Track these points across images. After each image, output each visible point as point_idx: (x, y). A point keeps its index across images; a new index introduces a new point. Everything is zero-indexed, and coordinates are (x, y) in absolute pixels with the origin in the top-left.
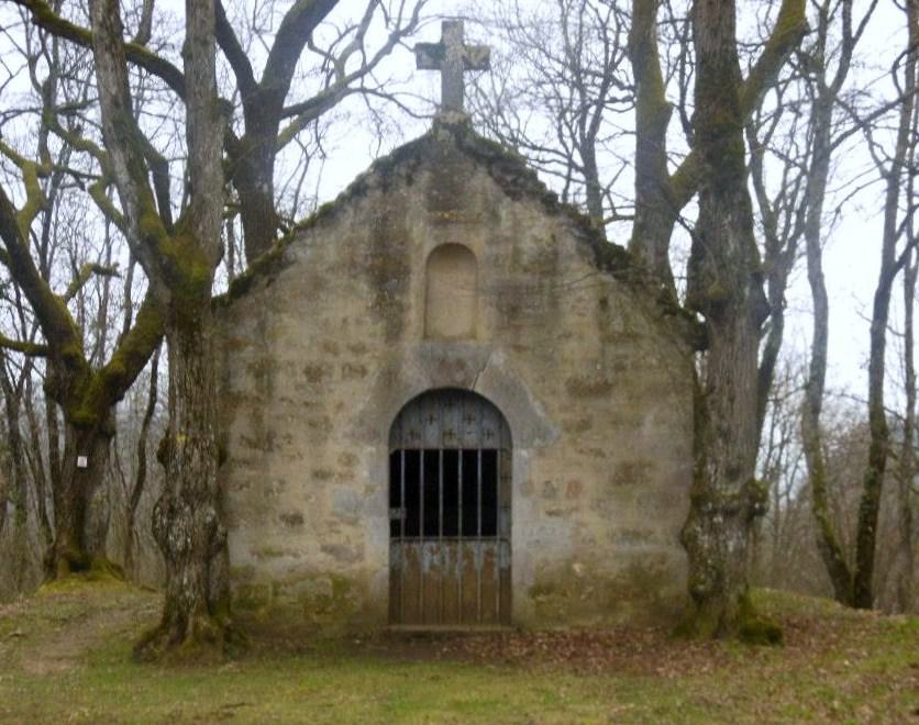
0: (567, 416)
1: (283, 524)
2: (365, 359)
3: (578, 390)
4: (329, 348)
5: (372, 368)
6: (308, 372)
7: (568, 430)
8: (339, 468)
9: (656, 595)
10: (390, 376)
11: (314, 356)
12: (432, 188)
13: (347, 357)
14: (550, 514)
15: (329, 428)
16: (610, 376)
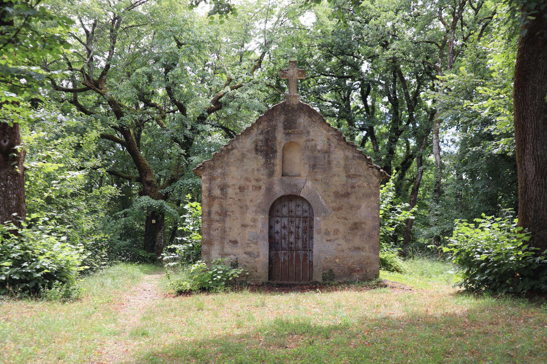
0: (334, 205)
1: (230, 244)
2: (261, 183)
3: (337, 195)
4: (247, 179)
5: (263, 187)
6: (240, 188)
7: (334, 210)
8: (251, 224)
9: (366, 271)
10: (269, 190)
11: (242, 183)
12: (285, 121)
13: (254, 183)
14: (327, 241)
15: (247, 209)
16: (349, 190)
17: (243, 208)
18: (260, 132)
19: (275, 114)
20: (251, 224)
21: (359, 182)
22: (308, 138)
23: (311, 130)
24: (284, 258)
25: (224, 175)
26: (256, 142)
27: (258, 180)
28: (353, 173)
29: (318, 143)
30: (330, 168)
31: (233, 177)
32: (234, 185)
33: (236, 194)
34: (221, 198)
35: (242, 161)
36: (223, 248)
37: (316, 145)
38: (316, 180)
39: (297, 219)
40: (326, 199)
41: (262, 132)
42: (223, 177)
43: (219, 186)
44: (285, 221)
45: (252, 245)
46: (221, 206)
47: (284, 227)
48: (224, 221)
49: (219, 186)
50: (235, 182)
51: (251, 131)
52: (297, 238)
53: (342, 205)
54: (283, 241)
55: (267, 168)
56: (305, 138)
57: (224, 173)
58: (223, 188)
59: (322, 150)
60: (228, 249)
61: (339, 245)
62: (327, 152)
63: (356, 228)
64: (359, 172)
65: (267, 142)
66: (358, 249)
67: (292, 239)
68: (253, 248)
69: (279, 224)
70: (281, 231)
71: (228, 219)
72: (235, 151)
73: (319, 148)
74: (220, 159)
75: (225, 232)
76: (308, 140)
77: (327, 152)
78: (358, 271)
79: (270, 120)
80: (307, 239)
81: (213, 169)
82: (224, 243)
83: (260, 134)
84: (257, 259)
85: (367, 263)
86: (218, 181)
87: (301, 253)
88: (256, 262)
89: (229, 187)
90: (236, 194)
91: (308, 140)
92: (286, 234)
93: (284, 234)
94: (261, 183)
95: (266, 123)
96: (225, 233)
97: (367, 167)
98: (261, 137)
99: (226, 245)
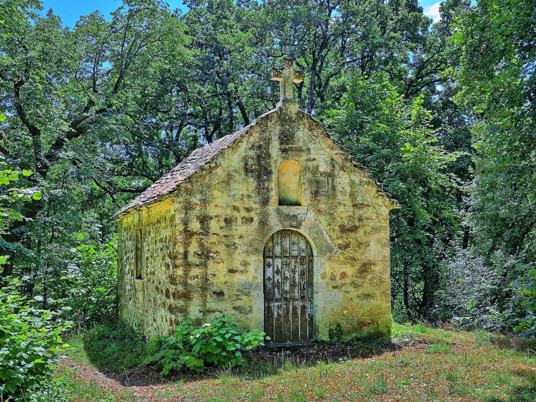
0: (340, 242)
1: (215, 296)
2: (252, 214)
3: (343, 229)
4: (236, 208)
5: (256, 218)
6: (225, 220)
7: (340, 248)
8: (242, 268)
9: (377, 323)
10: (263, 223)
11: (229, 212)
12: (282, 134)
13: (244, 213)
14: (334, 287)
15: (236, 248)
16: (357, 223)
17: (231, 247)
18: (250, 146)
19: (269, 125)
20: (242, 268)
21: (368, 213)
22: (309, 156)
23: (312, 148)
24: (278, 313)
25: (205, 202)
26: (245, 160)
27: (248, 210)
28: (361, 202)
29: (320, 163)
30: (334, 196)
31: (216, 206)
32: (217, 216)
33: (221, 228)
34: (202, 233)
35: (228, 184)
36: (205, 302)
37: (318, 167)
38: (319, 211)
39: (293, 261)
40: (331, 234)
41: (253, 146)
42: (203, 205)
43: (198, 217)
44: (278, 262)
45: (243, 297)
46: (201, 245)
47: (278, 272)
48: (205, 265)
49: (198, 217)
50: (218, 211)
51: (240, 144)
52: (293, 285)
53: (350, 242)
54: (276, 290)
55: (259, 194)
56: (304, 157)
57: (204, 200)
58: (204, 220)
59: (325, 173)
60: (211, 304)
61: (347, 292)
62: (331, 175)
63: (365, 271)
64: (366, 200)
65: (259, 161)
66: (368, 296)
67: (287, 288)
68: (244, 301)
69: (271, 267)
70: (274, 276)
71: (210, 263)
72: (219, 171)
73: (321, 169)
74: (200, 180)
75: (207, 280)
76: (309, 160)
77: (331, 175)
78: (369, 323)
79: (263, 131)
80: (305, 287)
81: (190, 195)
82: (206, 296)
83: (250, 149)
84: (249, 316)
85: (378, 314)
86: (197, 211)
87: (299, 304)
88: (248, 319)
89: (211, 218)
90: (221, 228)
91: (309, 160)
92: (280, 281)
93: (278, 281)
94: (252, 214)
95: (258, 135)
96: (207, 282)
97: (377, 195)
98: (252, 153)
99: (209, 299)
